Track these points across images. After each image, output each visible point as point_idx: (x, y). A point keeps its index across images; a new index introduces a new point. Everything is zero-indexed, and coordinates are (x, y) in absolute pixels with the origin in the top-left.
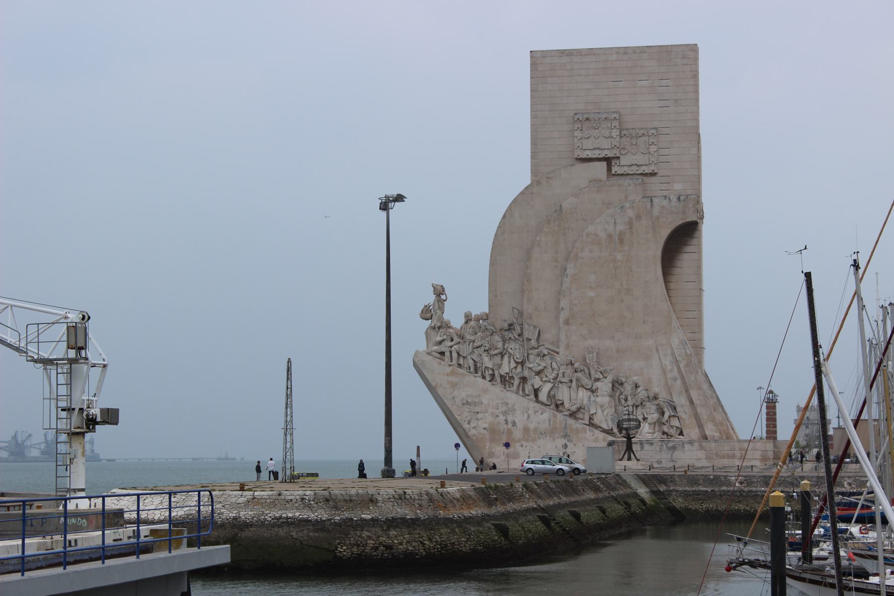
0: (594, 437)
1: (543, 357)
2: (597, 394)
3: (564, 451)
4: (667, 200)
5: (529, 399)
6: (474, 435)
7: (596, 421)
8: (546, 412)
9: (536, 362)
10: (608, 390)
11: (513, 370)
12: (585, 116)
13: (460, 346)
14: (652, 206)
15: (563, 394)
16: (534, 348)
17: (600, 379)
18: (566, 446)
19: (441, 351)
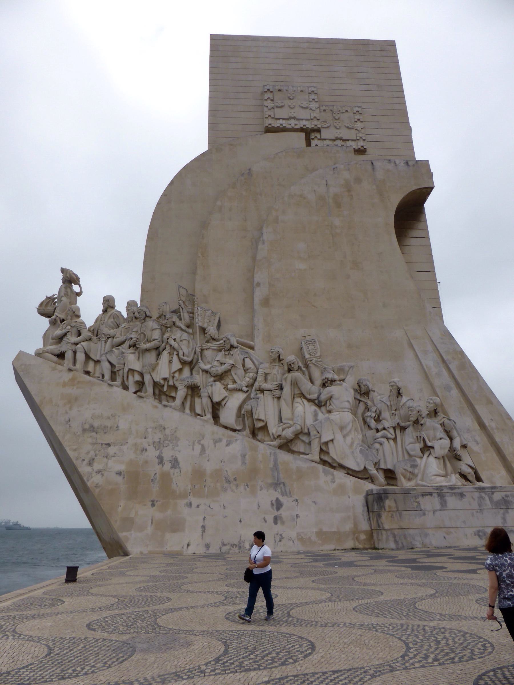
0: (335, 485)
3: (276, 513)
4: (393, 164)
6: (97, 486)
8: (236, 440)
13: (91, 344)
14: (373, 169)
16: (214, 339)
18: (278, 505)
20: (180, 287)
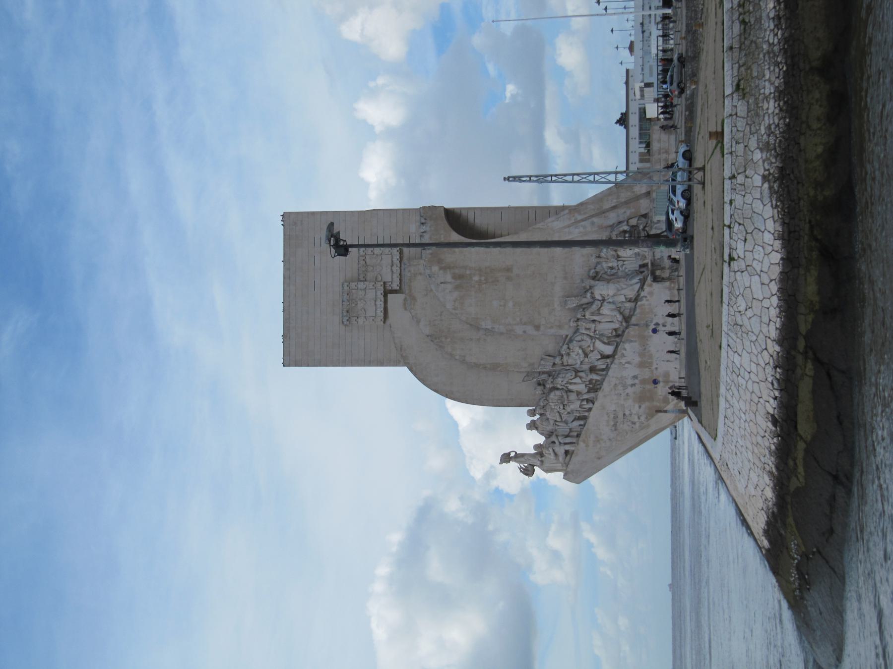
1: (570, 349)
2: (606, 296)
3: (661, 326)
4: (424, 234)
7: (632, 294)
11: (583, 380)
12: (345, 314)
15: (606, 328)
16: (562, 359)
19: (565, 455)
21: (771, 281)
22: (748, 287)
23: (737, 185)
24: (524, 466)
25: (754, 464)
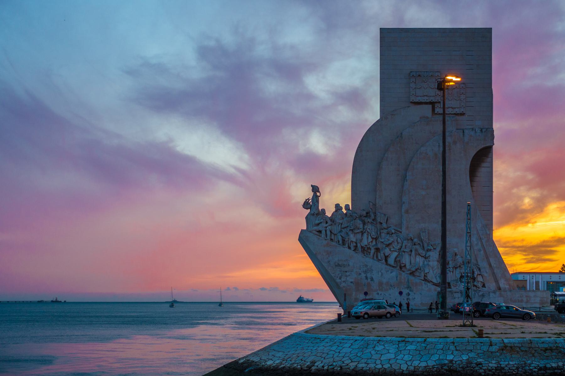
1: (391, 234)
3: (408, 297)
5: (382, 263)
6: (344, 287)
7: (429, 277)
9: (386, 238)
10: (437, 258)
11: (370, 243)
14: (464, 135)
15: (406, 259)
16: (385, 229)
17: (431, 250)
19: (318, 230)
20: (369, 202)
21: (391, 365)
22: (388, 351)
23: (449, 346)
24: (310, 202)
25: (287, 355)
